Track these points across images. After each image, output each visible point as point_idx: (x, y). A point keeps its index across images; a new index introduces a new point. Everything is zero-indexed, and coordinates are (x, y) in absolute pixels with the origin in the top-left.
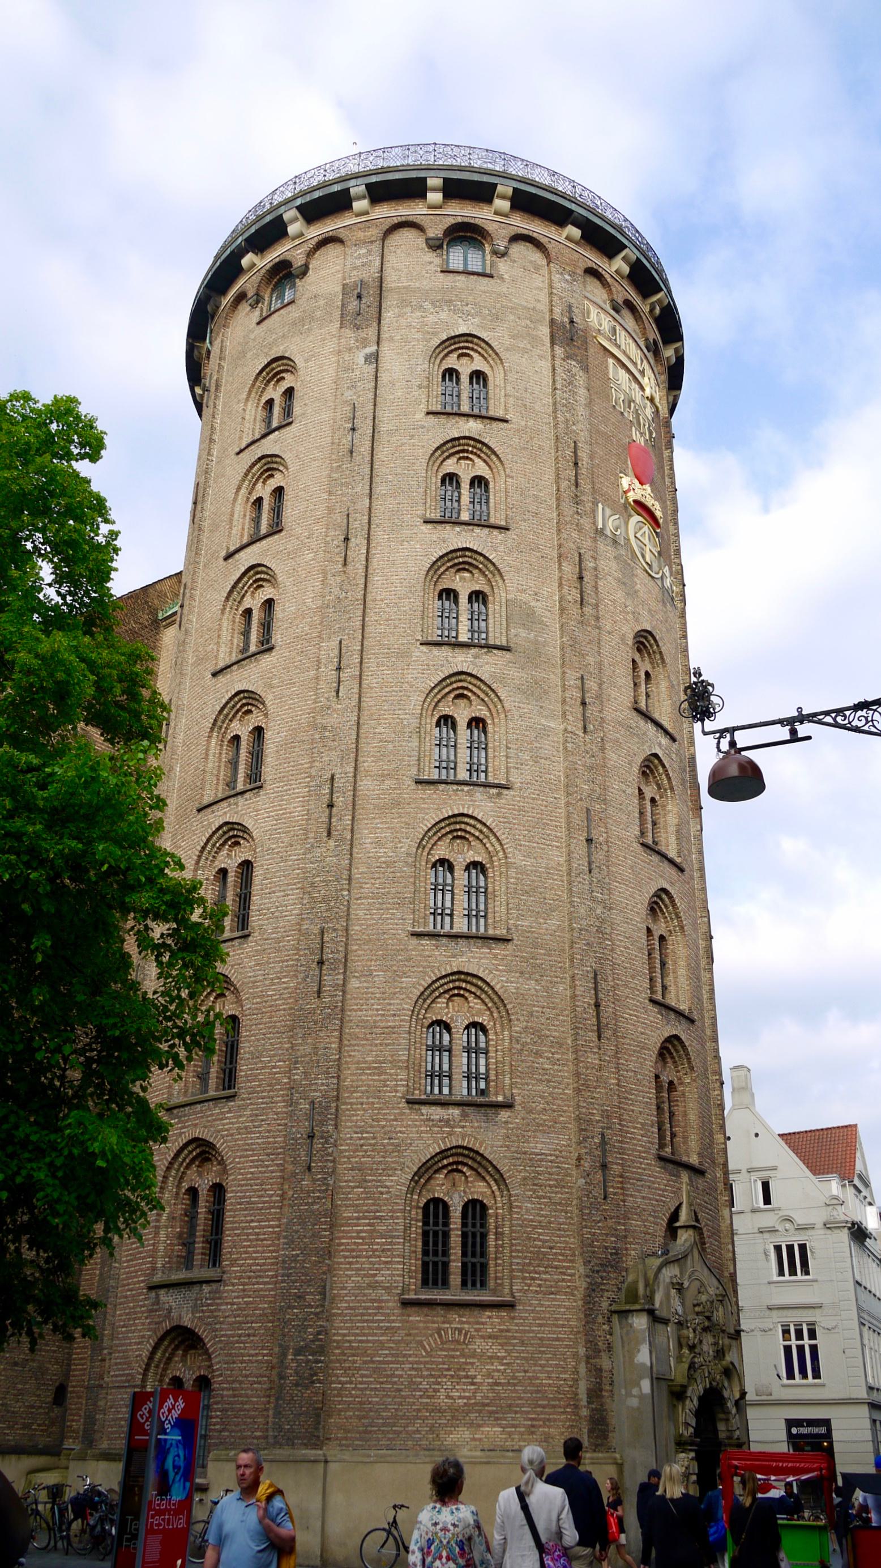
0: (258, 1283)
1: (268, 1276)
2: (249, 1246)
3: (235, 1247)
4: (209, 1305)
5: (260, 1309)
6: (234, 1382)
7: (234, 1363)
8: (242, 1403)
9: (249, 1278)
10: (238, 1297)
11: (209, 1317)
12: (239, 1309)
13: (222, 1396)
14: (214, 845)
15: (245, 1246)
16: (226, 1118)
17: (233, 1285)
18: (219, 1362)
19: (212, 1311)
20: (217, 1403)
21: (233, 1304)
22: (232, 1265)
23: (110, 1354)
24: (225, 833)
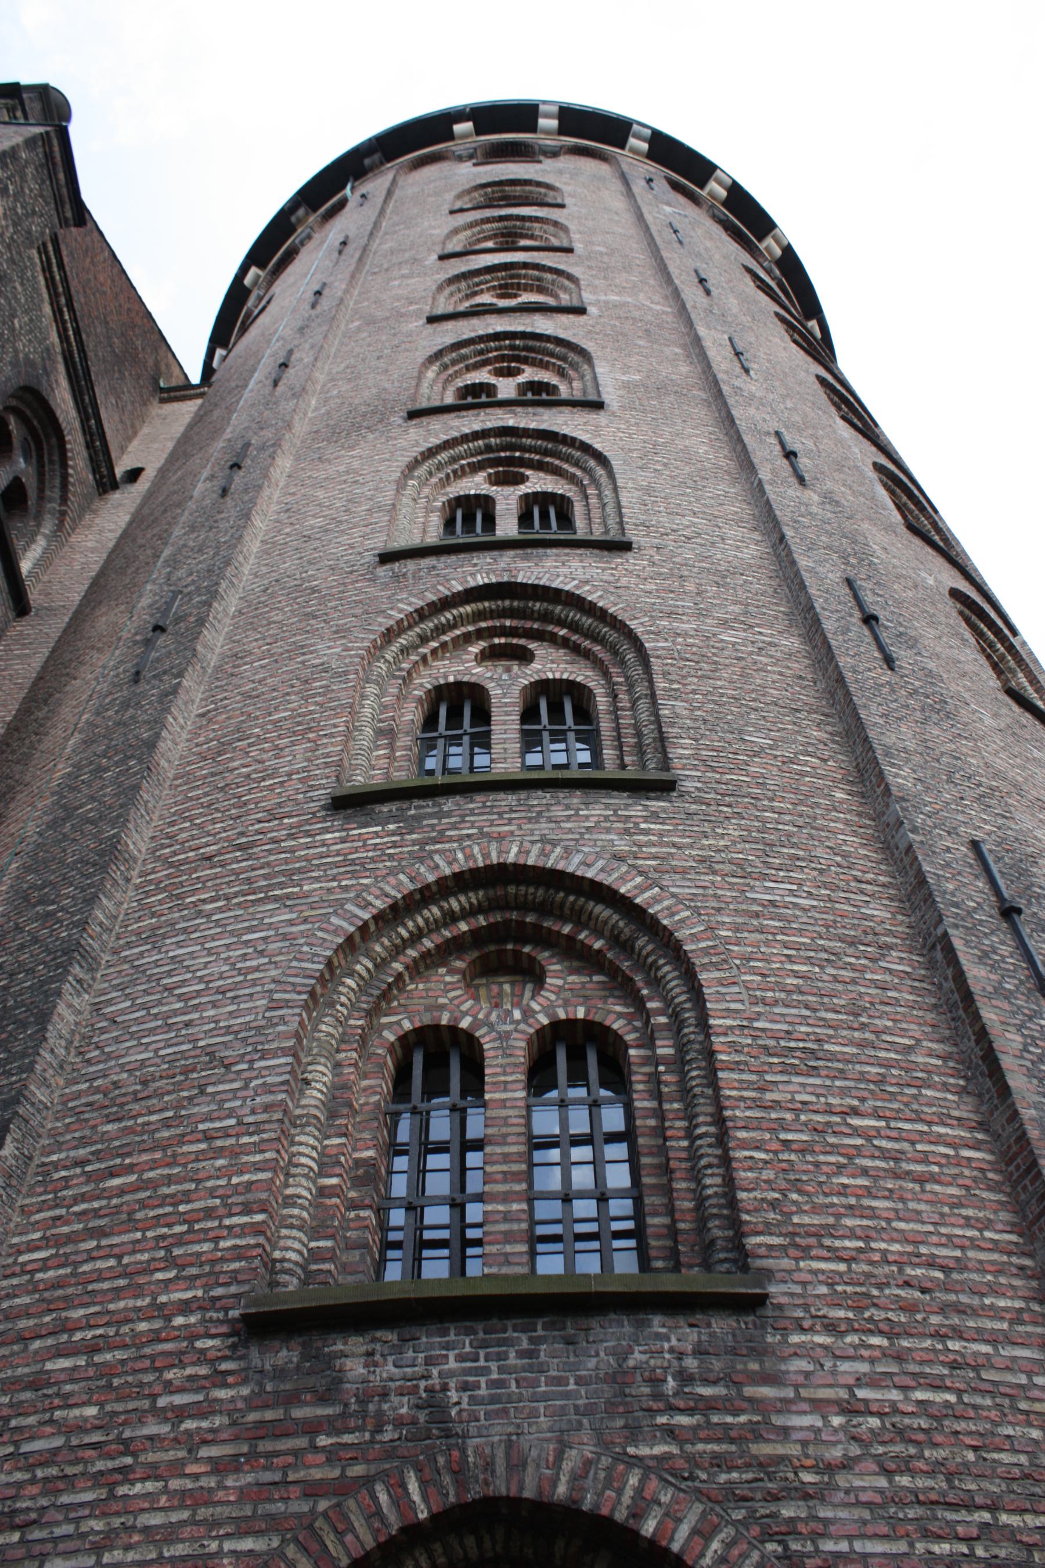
0: (959, 1334)
1: (996, 1313)
2: (868, 1192)
3: (796, 1185)
4: (709, 1406)
5: (1011, 1444)
9: (910, 1308)
10: (873, 1382)
11: (719, 1463)
12: (902, 1434)
14: (454, 460)
15: (844, 1190)
16: (647, 832)
17: (831, 1327)
19: (726, 1434)
21: (851, 1409)
22: (806, 1252)
24: (489, 448)
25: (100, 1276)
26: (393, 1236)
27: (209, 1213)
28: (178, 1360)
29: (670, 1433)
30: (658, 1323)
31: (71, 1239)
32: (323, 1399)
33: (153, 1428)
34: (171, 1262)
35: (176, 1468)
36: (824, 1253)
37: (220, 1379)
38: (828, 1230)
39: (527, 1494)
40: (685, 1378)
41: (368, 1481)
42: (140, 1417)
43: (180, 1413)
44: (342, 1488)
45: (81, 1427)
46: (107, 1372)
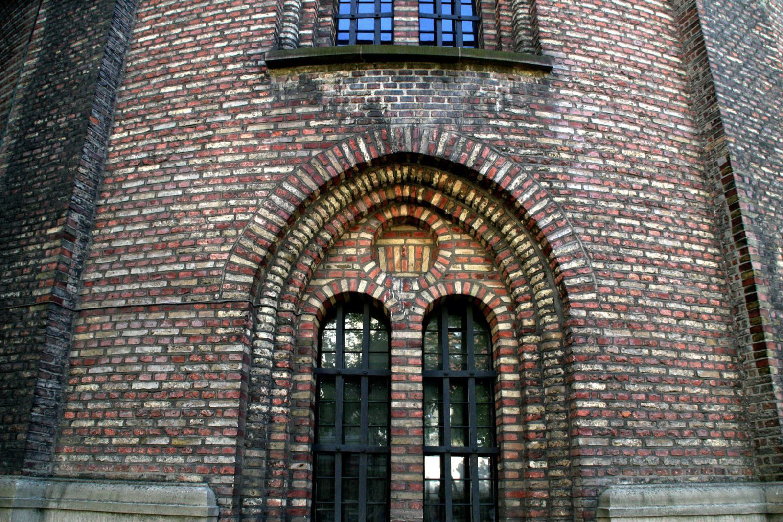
2: (607, 26)
3: (570, 17)
4: (518, 118)
5: (663, 153)
6: (628, 308)
7: (622, 260)
8: (661, 362)
9: (623, 85)
10: (601, 116)
12: (612, 142)
13: (601, 342)
15: (594, 23)
17: (582, 88)
18: (574, 256)
20: (590, 358)
22: (572, 51)
23: (87, 228)
25: (184, 46)
26: (341, 37)
27: (243, 13)
28: (232, 85)
29: (496, 129)
30: (492, 76)
31: (165, 29)
32: (312, 104)
33: (221, 118)
34: (223, 38)
35: (237, 136)
36: (582, 52)
37: (256, 94)
38: (585, 42)
39: (422, 152)
40: (506, 104)
41: (338, 143)
42: (214, 113)
43: (236, 111)
44: (325, 146)
45: (184, 118)
46: (194, 93)
